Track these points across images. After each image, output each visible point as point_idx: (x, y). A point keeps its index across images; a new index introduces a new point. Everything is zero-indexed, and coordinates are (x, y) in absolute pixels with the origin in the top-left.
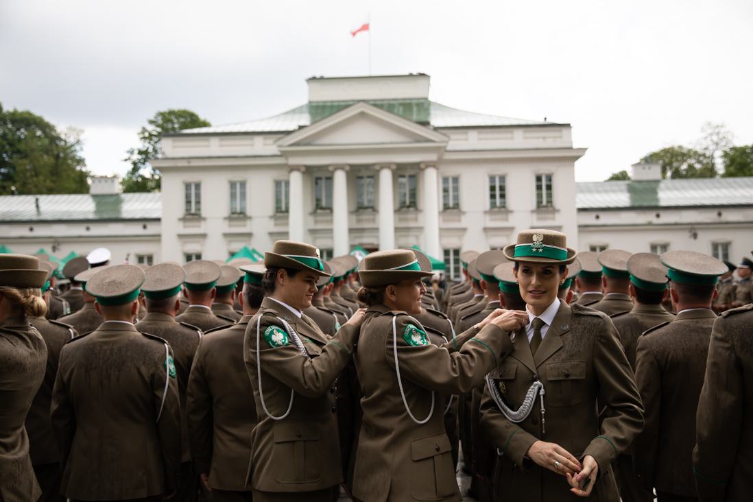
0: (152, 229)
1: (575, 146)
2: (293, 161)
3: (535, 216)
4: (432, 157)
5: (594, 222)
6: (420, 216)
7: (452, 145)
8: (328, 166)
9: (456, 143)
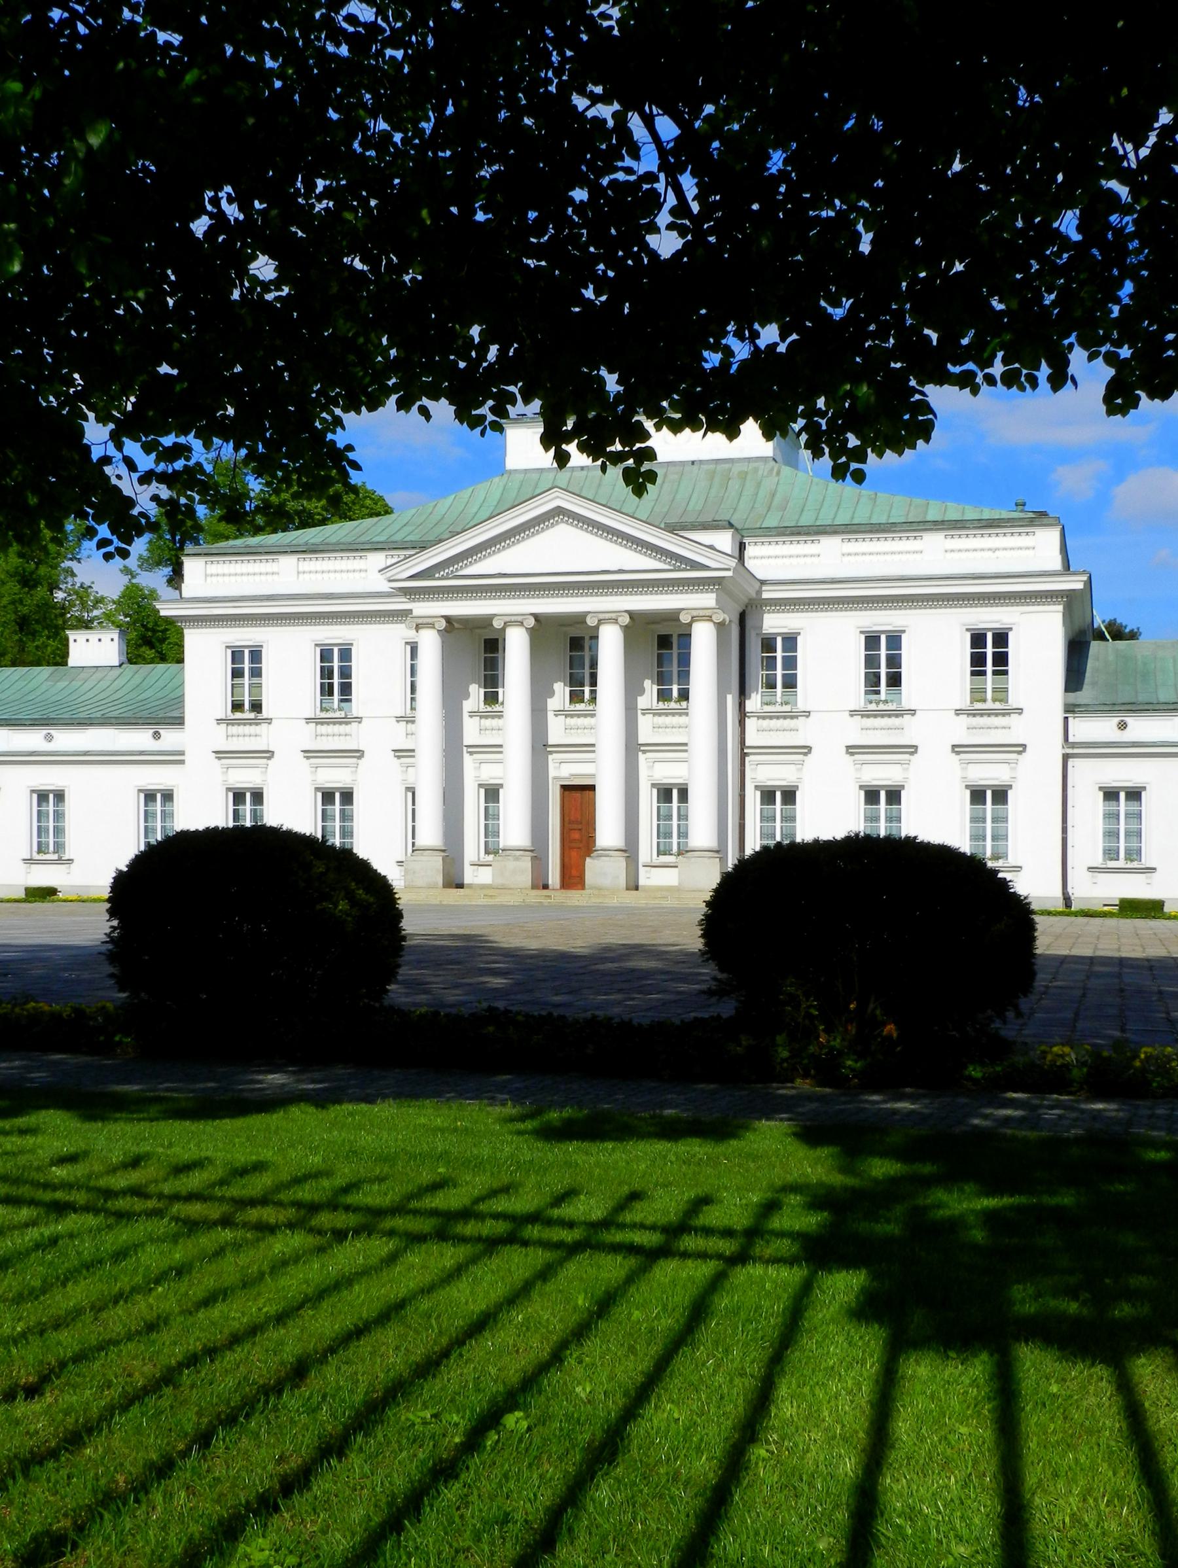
0: (170, 738)
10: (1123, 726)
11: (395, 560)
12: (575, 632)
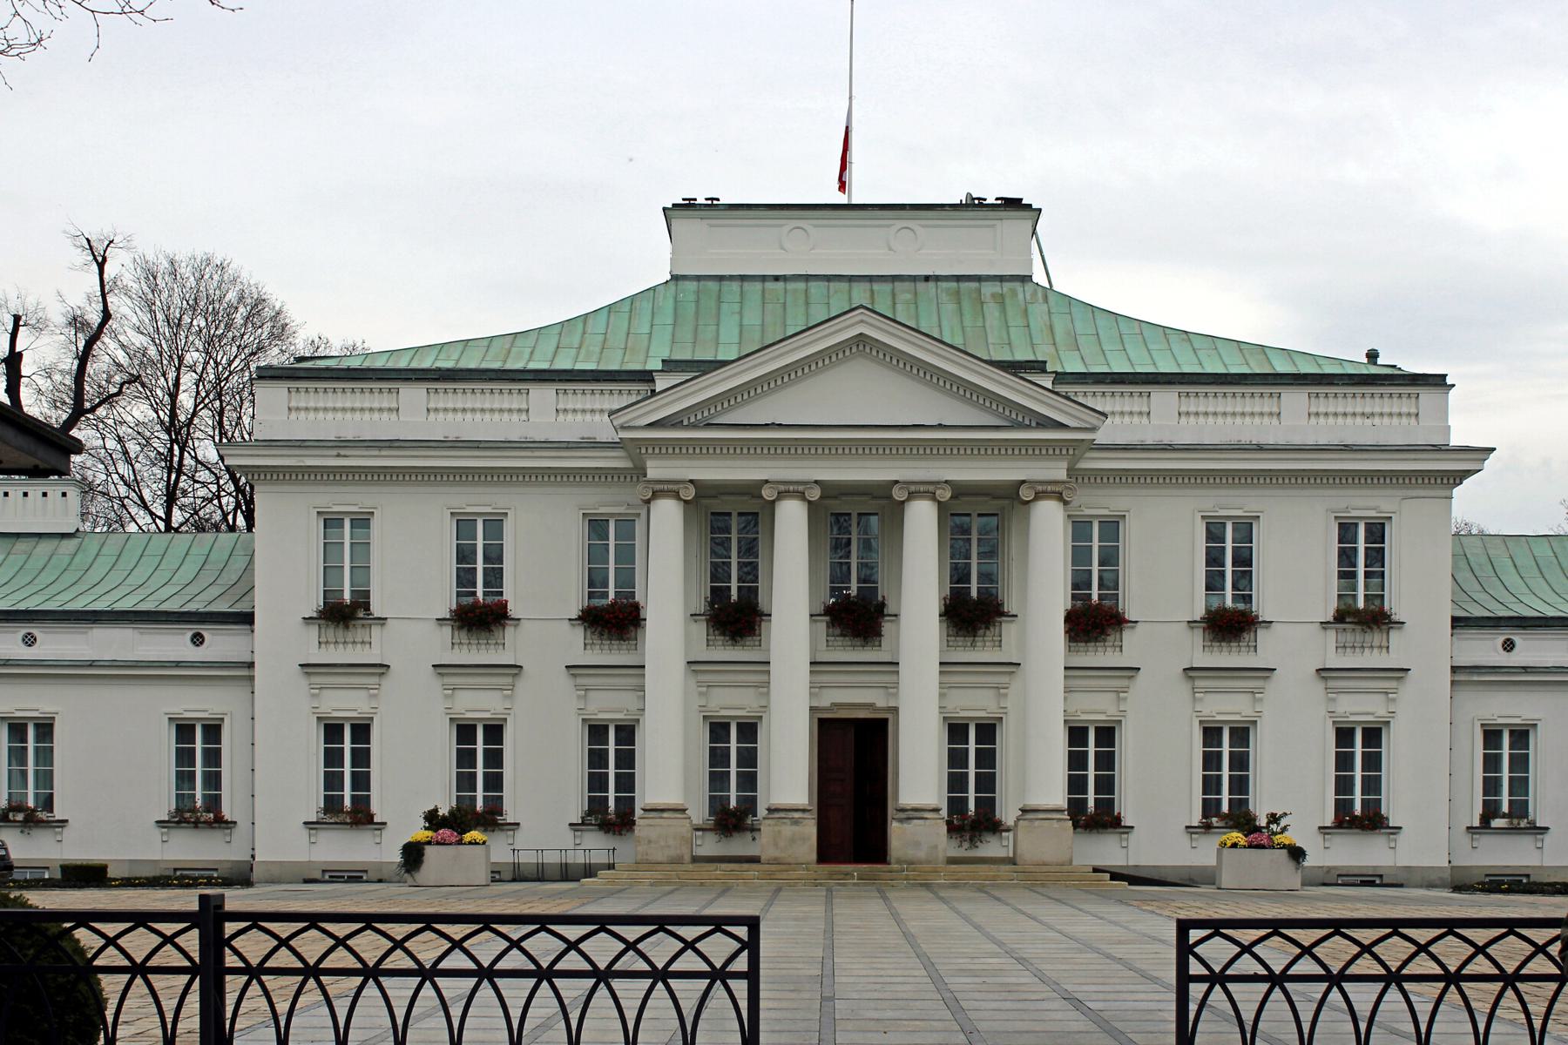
0: (221, 644)
1: (1455, 441)
2: (656, 470)
4: (1056, 471)
10: (1509, 646)
11: (634, 399)
12: (750, 506)
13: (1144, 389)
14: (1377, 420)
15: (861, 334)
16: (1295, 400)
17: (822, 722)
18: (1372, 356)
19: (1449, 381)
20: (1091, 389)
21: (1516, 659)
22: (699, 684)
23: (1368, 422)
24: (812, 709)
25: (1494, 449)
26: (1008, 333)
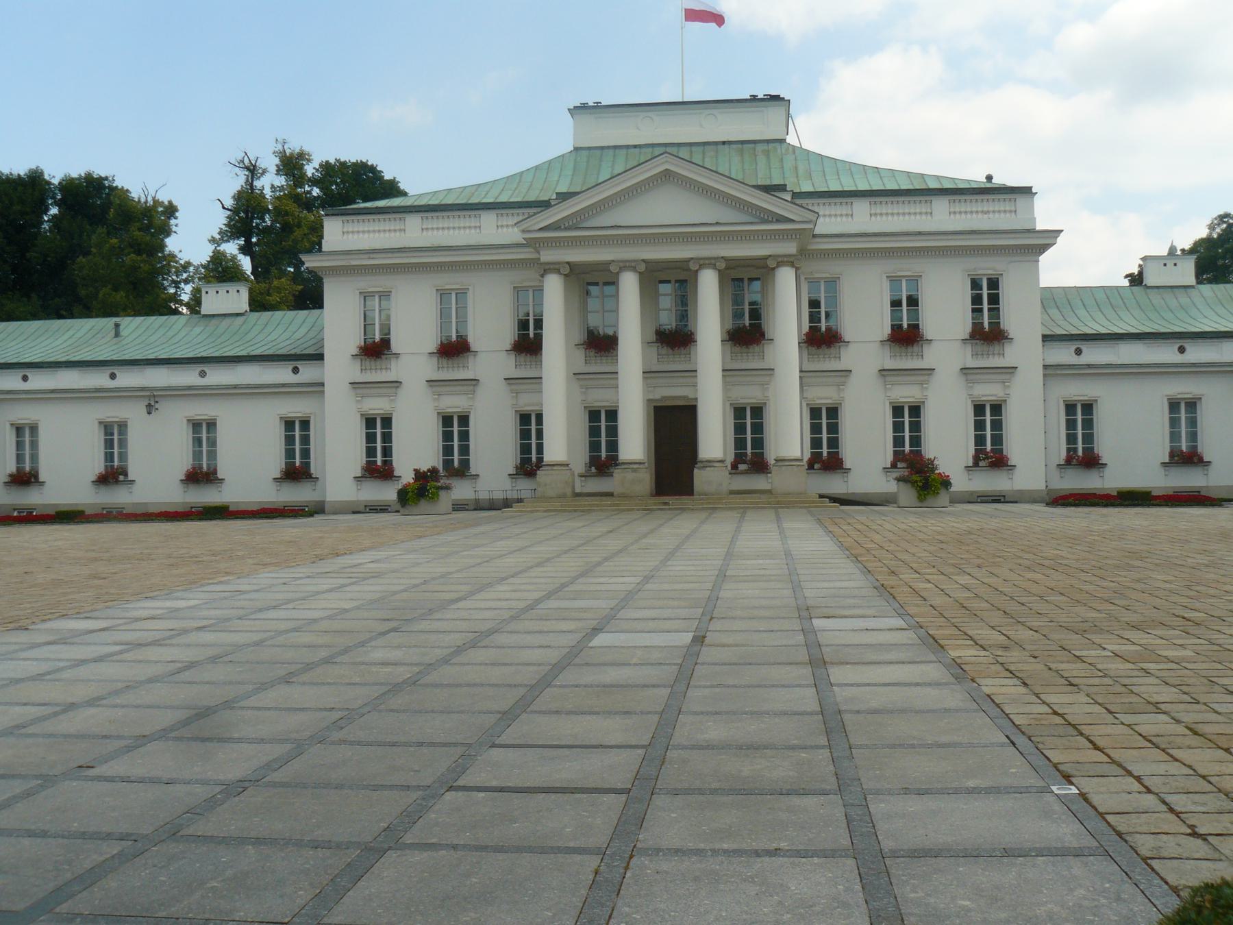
0: (308, 373)
1: (1040, 226)
2: (547, 256)
3: (969, 349)
4: (790, 248)
5: (1073, 359)
6: (768, 349)
7: (823, 227)
8: (608, 263)
9: (831, 221)
10: (1078, 352)
13: (849, 200)
14: (991, 215)
15: (667, 170)
16: (941, 206)
17: (655, 407)
18: (989, 178)
19: (1034, 191)
20: (816, 201)
21: (1085, 358)
22: (581, 387)
23: (986, 216)
24: (649, 401)
25: (1062, 231)
26: (770, 171)
